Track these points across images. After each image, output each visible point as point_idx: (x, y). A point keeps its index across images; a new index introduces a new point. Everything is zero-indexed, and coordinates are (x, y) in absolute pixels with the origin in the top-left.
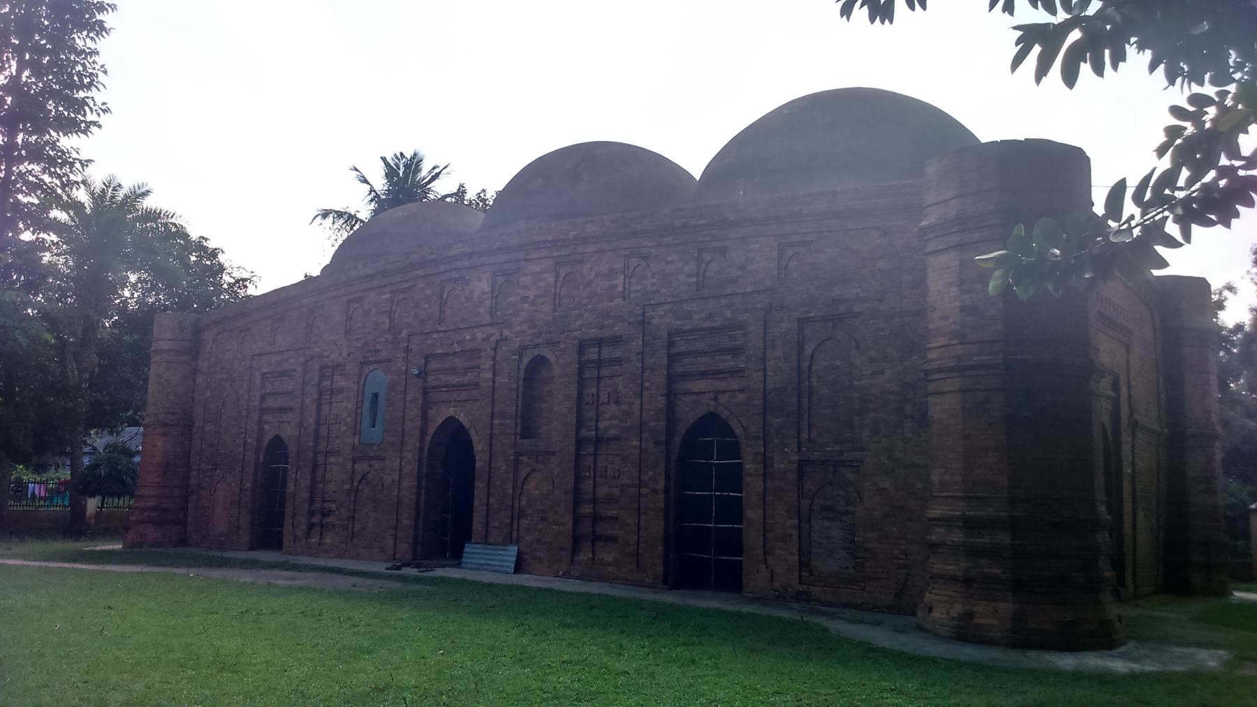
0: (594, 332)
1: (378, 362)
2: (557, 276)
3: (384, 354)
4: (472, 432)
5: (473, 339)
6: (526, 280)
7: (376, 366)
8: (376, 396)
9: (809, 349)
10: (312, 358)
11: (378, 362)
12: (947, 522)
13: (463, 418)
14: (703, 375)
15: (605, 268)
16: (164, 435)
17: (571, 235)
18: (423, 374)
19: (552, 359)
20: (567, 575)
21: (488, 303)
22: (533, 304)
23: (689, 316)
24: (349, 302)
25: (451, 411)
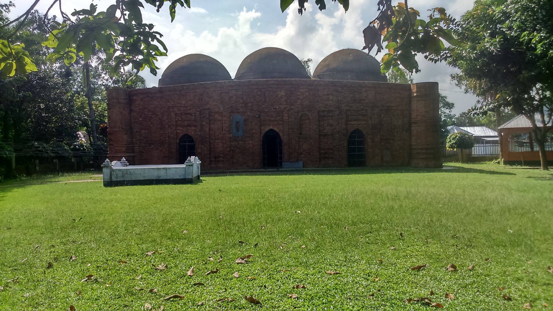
0: (323, 109)
2: (309, 94)
3: (241, 110)
4: (281, 134)
6: (298, 93)
9: (382, 116)
12: (422, 149)
13: (275, 129)
14: (355, 120)
15: (326, 93)
16: (126, 134)
18: (260, 116)
19: (310, 115)
20: (318, 167)
21: (284, 98)
22: (301, 100)
23: (352, 107)
25: (271, 127)
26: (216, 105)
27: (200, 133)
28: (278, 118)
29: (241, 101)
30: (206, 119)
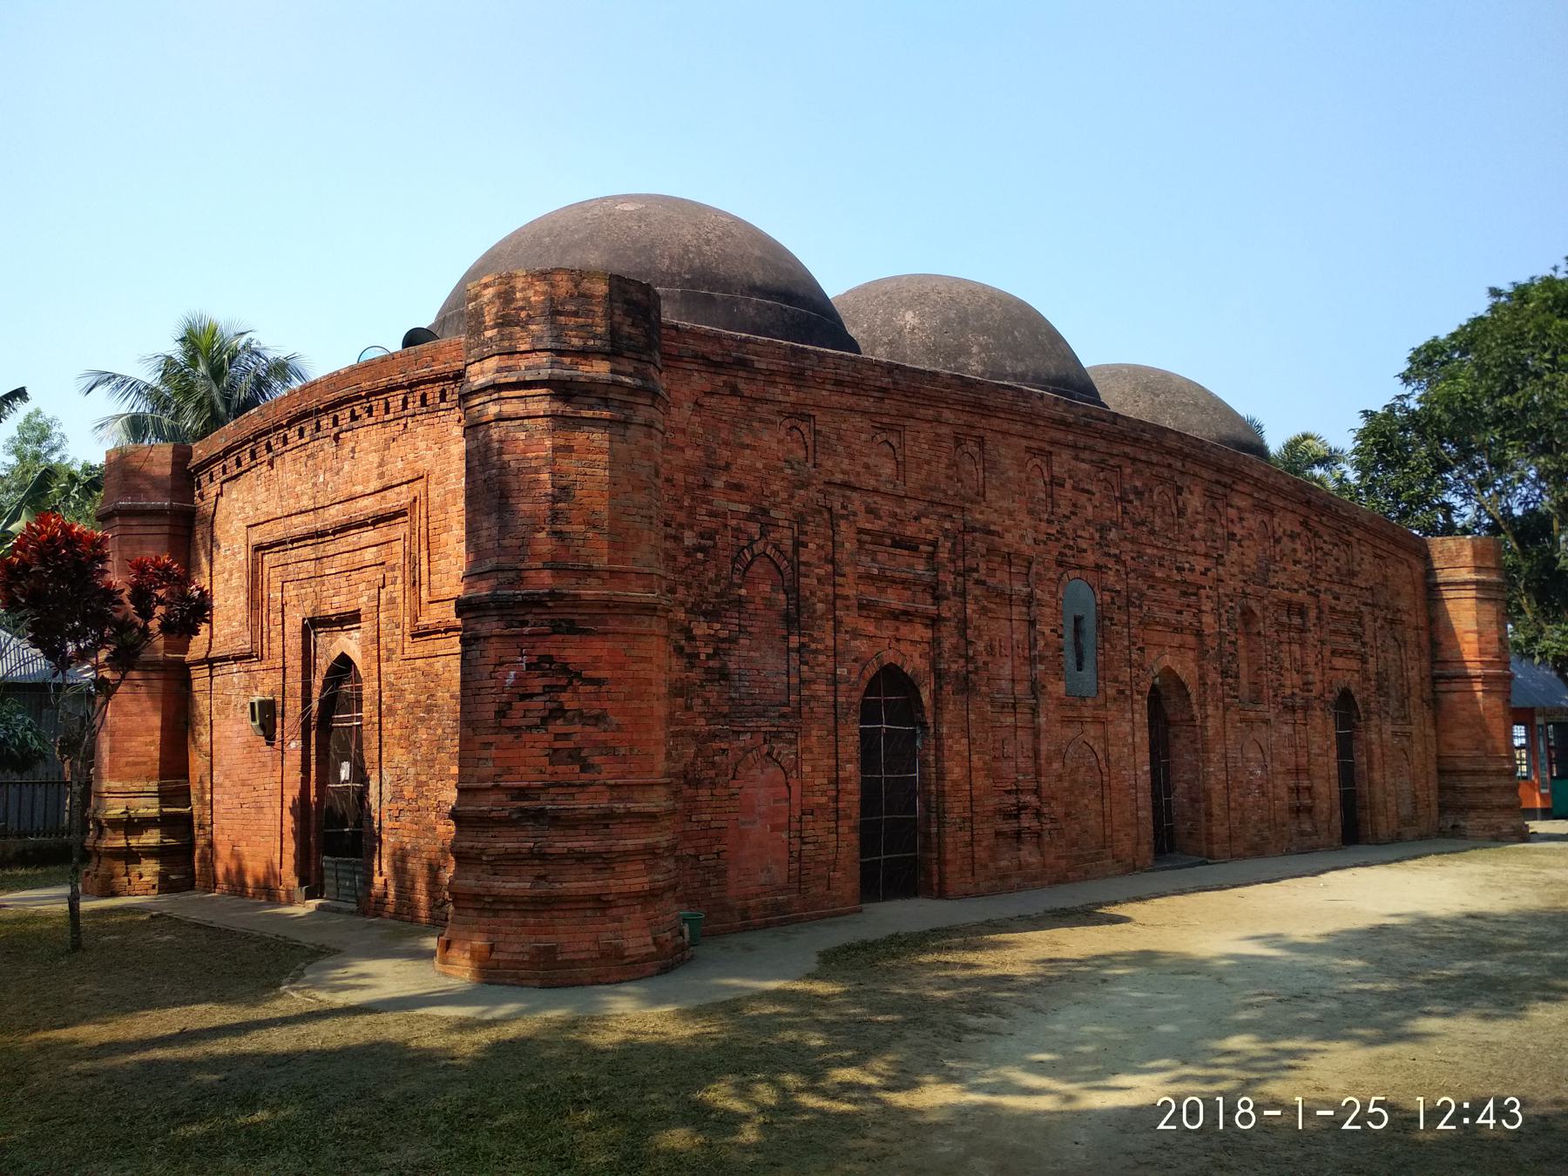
1: (1080, 567)
3: (1090, 558)
5: (1192, 570)
7: (1077, 573)
8: (1078, 620)
10: (974, 530)
11: (1080, 567)
17: (1271, 480)
24: (1028, 449)
25: (1167, 660)
26: (1011, 514)
27: (954, 667)
28: (1187, 617)
29: (1090, 509)
30: (977, 582)
